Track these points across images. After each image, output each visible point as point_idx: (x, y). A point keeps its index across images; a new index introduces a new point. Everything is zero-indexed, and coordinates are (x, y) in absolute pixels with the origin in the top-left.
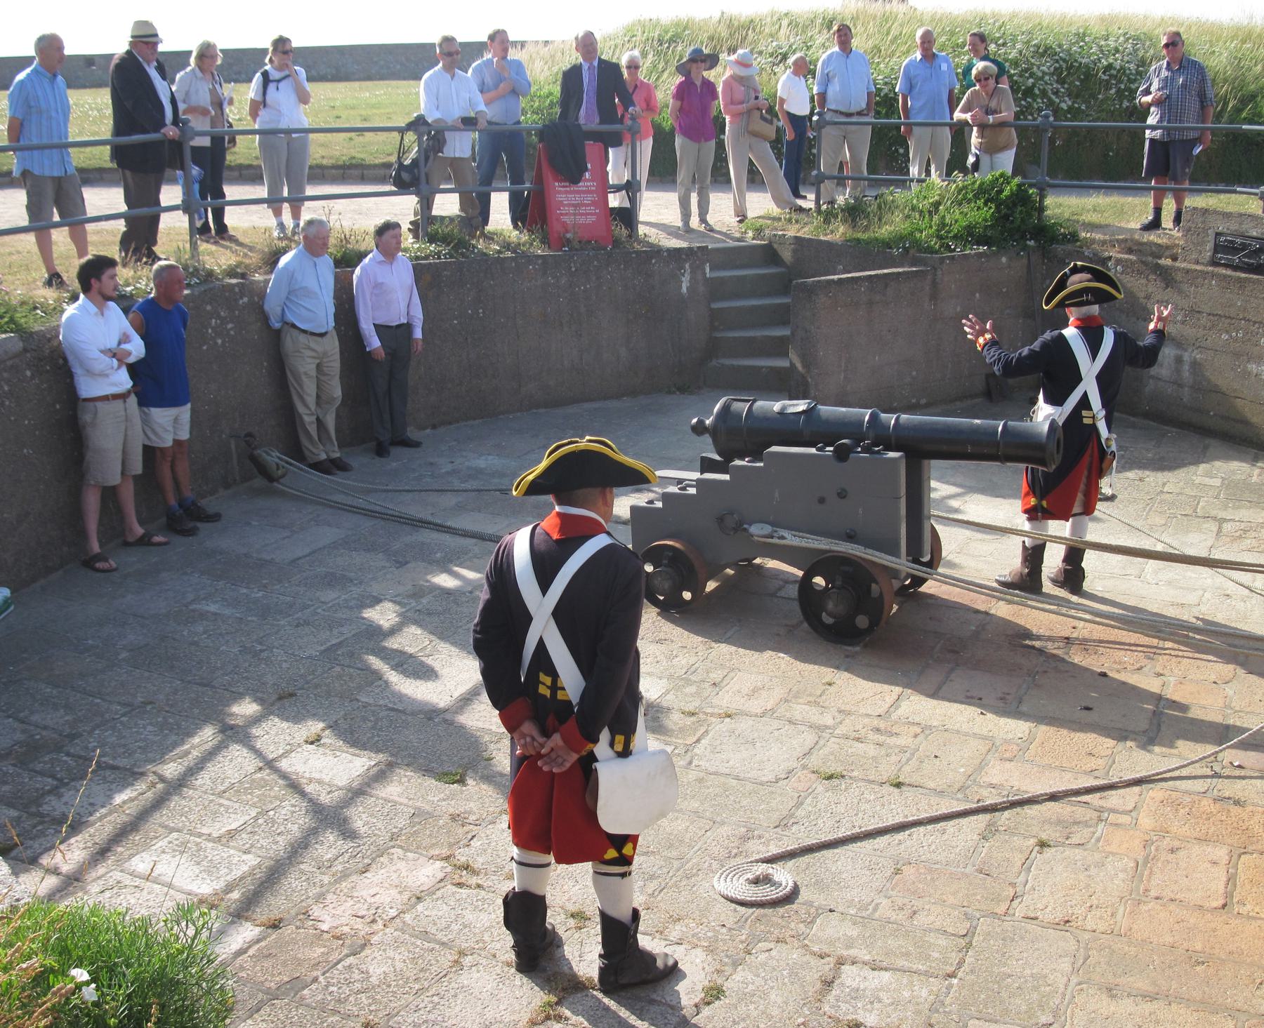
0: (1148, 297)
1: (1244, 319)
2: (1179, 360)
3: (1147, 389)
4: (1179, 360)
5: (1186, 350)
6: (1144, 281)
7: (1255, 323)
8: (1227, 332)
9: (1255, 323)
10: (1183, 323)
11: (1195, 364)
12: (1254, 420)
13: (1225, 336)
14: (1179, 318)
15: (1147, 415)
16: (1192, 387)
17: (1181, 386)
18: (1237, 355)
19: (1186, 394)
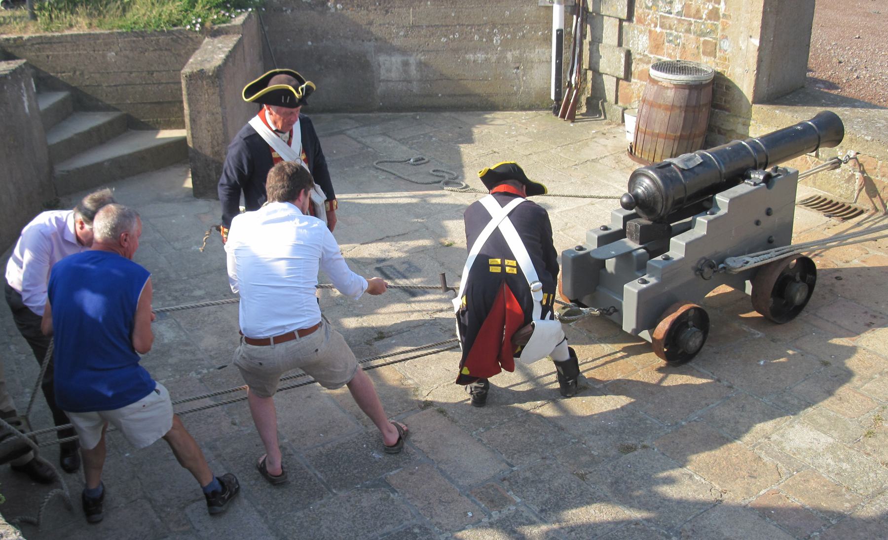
0: (371, 23)
1: (459, 24)
2: (406, 64)
3: (379, 91)
4: (406, 64)
5: (411, 55)
6: (365, 12)
7: (468, 25)
8: (445, 36)
9: (468, 25)
10: (405, 36)
11: (420, 64)
12: (477, 91)
13: (443, 40)
14: (402, 33)
15: (381, 109)
16: (420, 80)
17: (410, 82)
18: (455, 51)
19: (415, 88)
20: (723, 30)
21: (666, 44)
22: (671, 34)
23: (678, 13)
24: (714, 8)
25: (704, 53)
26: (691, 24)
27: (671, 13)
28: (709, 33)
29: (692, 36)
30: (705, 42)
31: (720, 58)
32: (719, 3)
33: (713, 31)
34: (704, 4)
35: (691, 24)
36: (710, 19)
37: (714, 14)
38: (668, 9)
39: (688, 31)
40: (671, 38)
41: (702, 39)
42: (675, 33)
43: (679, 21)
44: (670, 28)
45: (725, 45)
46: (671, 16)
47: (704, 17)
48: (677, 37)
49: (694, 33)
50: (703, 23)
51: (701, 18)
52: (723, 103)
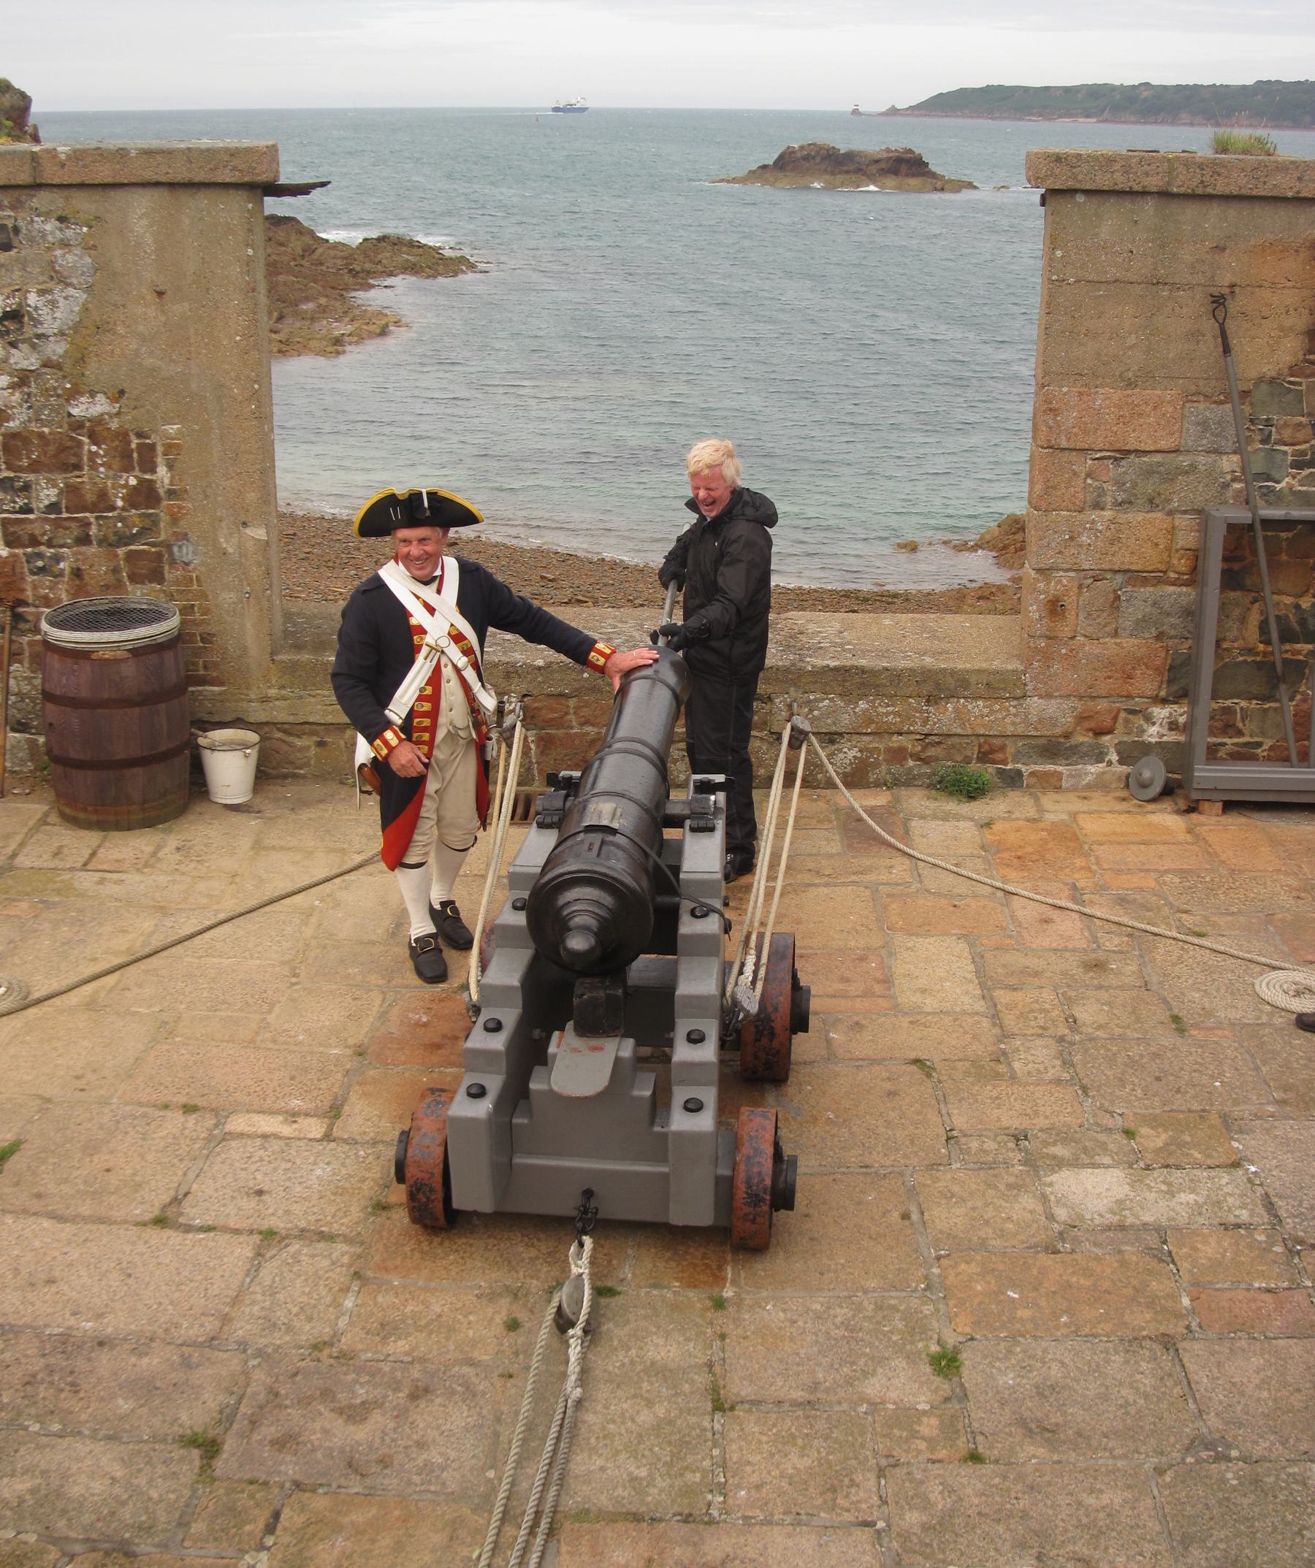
20: (175, 520)
21: (30, 578)
22: (40, 556)
23: (53, 507)
24: (141, 481)
25: (134, 578)
26: (89, 524)
27: (30, 511)
28: (140, 534)
29: (92, 550)
30: (130, 556)
31: (177, 582)
32: (153, 471)
33: (149, 527)
34: (116, 477)
35: (89, 524)
36: (134, 506)
37: (145, 495)
38: (20, 502)
39: (84, 540)
40: (40, 564)
41: (121, 552)
42: (49, 552)
43: (57, 524)
44: (34, 542)
45: (185, 552)
46: (31, 516)
47: (120, 503)
48: (57, 559)
49: (100, 543)
50: (121, 519)
51: (113, 508)
52: (202, 672)
